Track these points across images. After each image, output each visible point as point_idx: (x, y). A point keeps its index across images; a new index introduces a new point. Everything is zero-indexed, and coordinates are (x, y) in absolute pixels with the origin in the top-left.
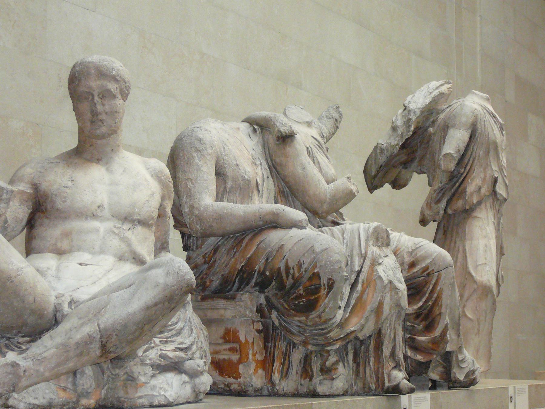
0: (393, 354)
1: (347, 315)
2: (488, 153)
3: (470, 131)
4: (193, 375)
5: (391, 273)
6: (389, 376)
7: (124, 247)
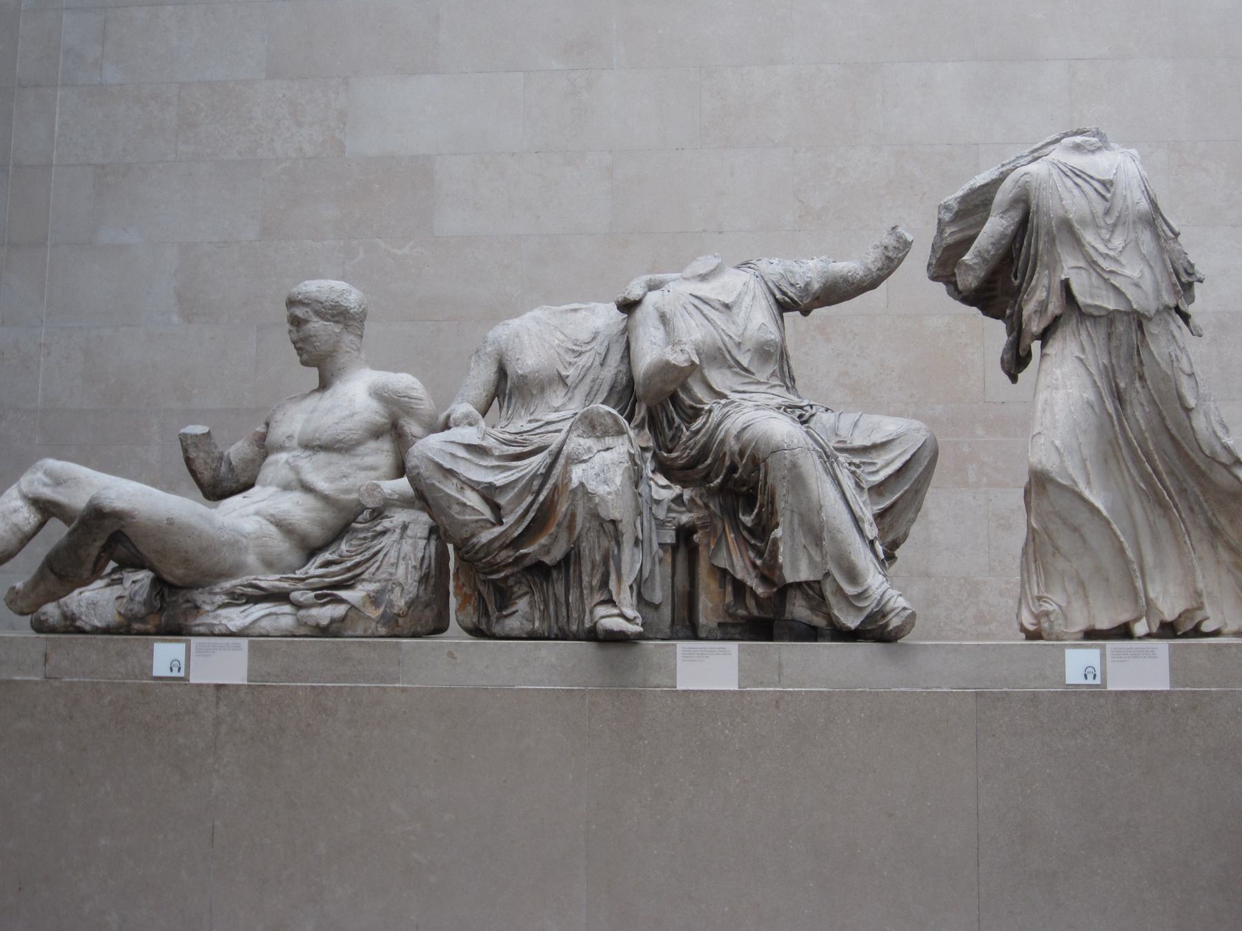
0: (604, 584)
1: (516, 534)
2: (1052, 240)
3: (1016, 215)
4: (298, 606)
5: (592, 472)
6: (591, 612)
7: (291, 476)
